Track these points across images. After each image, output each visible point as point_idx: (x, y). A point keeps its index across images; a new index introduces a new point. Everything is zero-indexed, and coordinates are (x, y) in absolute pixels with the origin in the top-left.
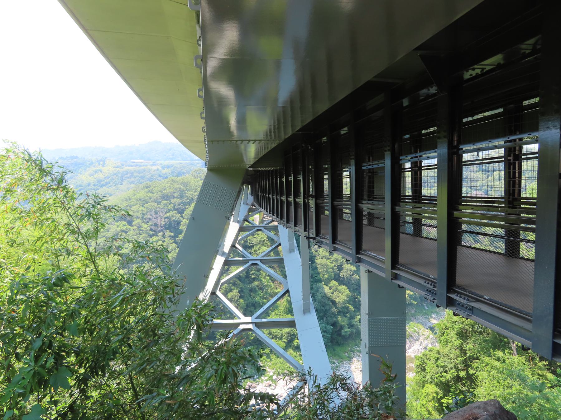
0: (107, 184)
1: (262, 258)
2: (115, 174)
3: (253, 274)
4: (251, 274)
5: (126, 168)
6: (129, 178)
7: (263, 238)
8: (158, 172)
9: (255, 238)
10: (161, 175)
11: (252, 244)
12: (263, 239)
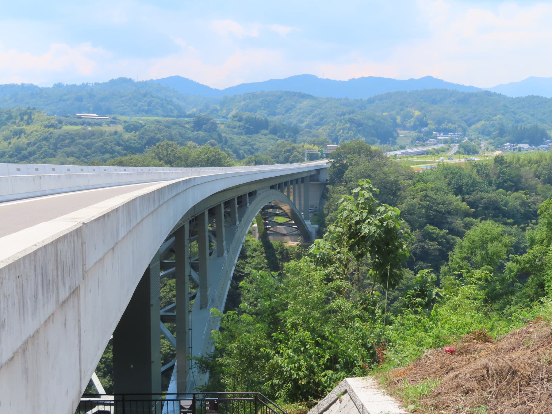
0: (31, 154)
1: (164, 314)
2: (46, 139)
5: (67, 128)
6: (66, 146)
8: (116, 137)
9: (247, 263)
10: (121, 142)
11: (242, 272)
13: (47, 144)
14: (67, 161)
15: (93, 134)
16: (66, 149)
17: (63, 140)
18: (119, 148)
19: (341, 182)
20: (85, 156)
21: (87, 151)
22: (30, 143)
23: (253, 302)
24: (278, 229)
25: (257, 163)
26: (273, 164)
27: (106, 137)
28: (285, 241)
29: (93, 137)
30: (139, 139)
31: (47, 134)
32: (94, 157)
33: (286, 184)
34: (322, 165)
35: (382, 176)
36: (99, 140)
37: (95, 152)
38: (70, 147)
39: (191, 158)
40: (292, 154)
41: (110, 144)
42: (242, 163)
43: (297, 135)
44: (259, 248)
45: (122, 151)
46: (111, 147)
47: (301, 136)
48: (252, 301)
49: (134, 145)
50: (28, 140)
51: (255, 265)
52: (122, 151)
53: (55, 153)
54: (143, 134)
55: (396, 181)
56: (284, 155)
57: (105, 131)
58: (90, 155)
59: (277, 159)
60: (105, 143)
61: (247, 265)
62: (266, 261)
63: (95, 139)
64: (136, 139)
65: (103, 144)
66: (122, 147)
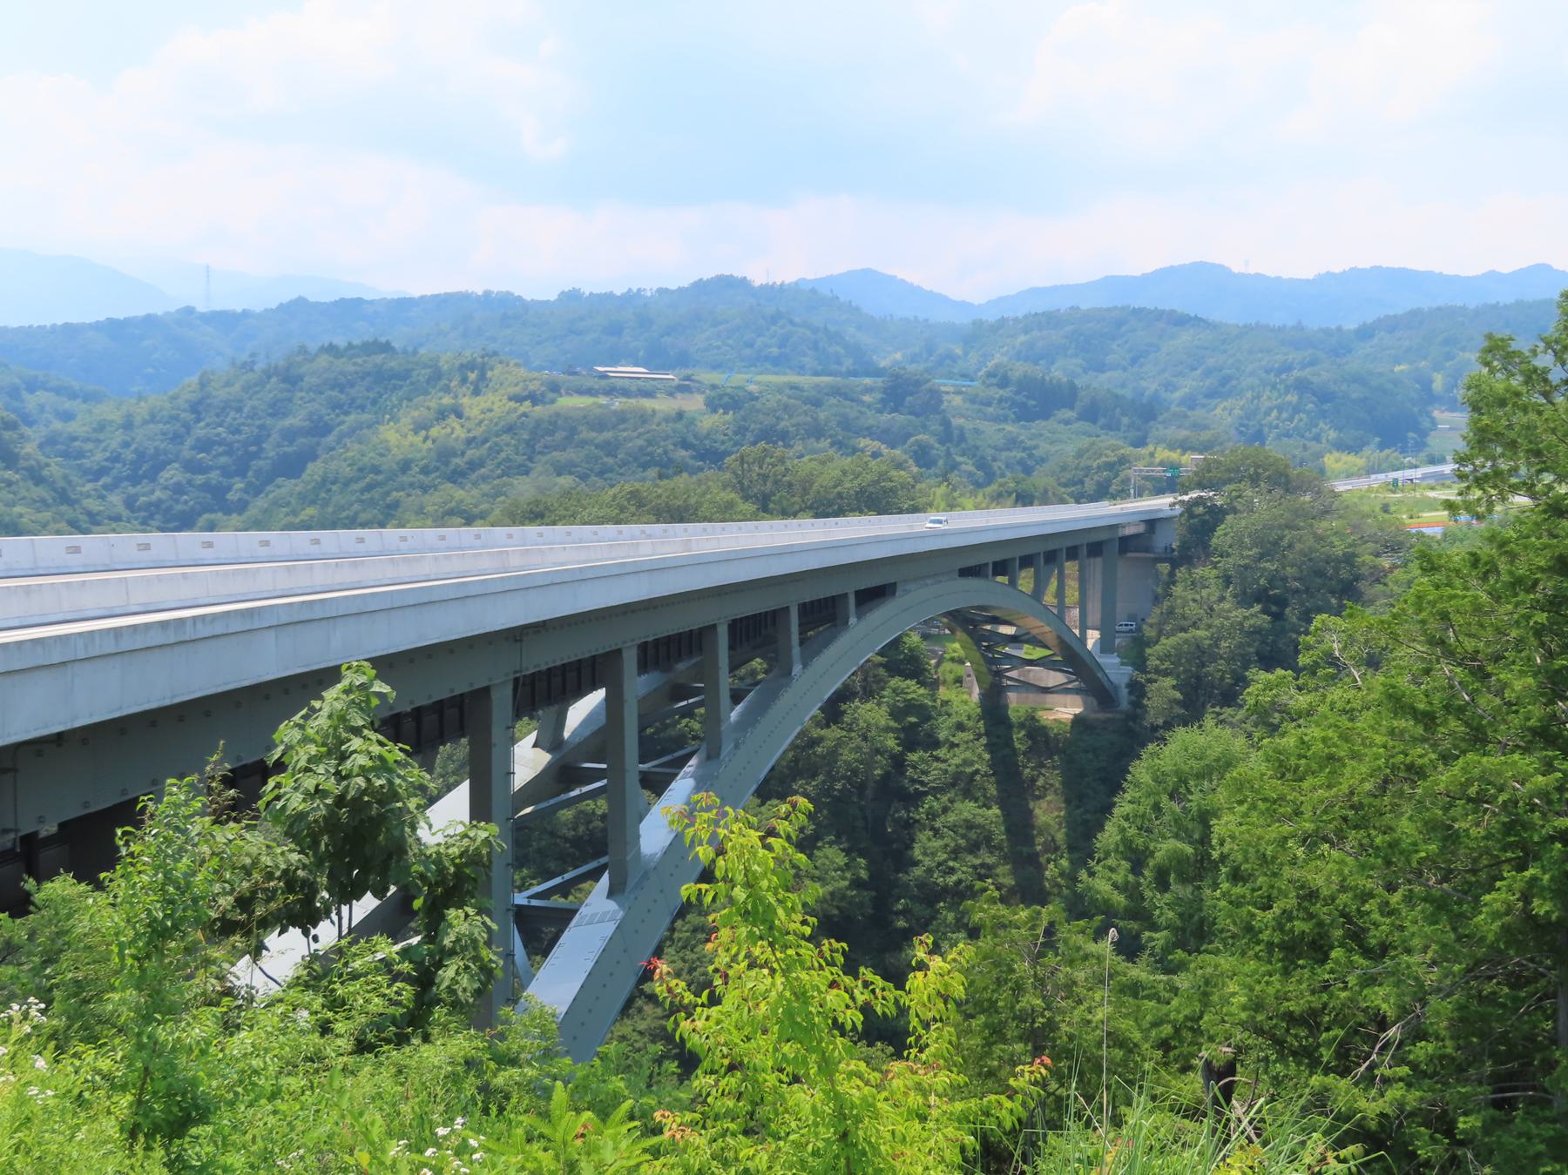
0: (473, 466)
2: (510, 429)
3: (905, 912)
4: (898, 913)
5: (569, 403)
6: (556, 448)
7: (972, 763)
8: (679, 426)
9: (937, 759)
10: (691, 439)
11: (922, 783)
12: (969, 770)
13: (513, 442)
14: (556, 484)
15: (621, 417)
16: (555, 454)
17: (551, 433)
18: (684, 453)
19: (1208, 555)
20: (601, 474)
21: (606, 459)
22: (474, 438)
23: (945, 861)
24: (1031, 674)
25: (1024, 499)
26: (1062, 501)
27: (654, 427)
28: (1047, 706)
29: (622, 426)
30: (736, 433)
31: (514, 416)
32: (622, 474)
33: (1051, 557)
34: (1160, 510)
35: (1311, 542)
36: (635, 434)
37: (624, 464)
38: (564, 450)
39: (816, 487)
40: (1116, 476)
41: (662, 443)
42: (980, 497)
43: (1152, 423)
44: (971, 724)
45: (691, 462)
46: (666, 452)
47: (1160, 426)
48: (941, 859)
49: (723, 447)
50: (469, 431)
51: (957, 766)
52: (691, 462)
53: (530, 464)
54: (745, 421)
55: (1349, 559)
56: (1096, 478)
57: (654, 411)
58: (611, 470)
59: (1079, 487)
60: (650, 443)
61: (935, 764)
62: (987, 756)
63: (624, 430)
64: (730, 432)
65: (645, 444)
66: (690, 452)
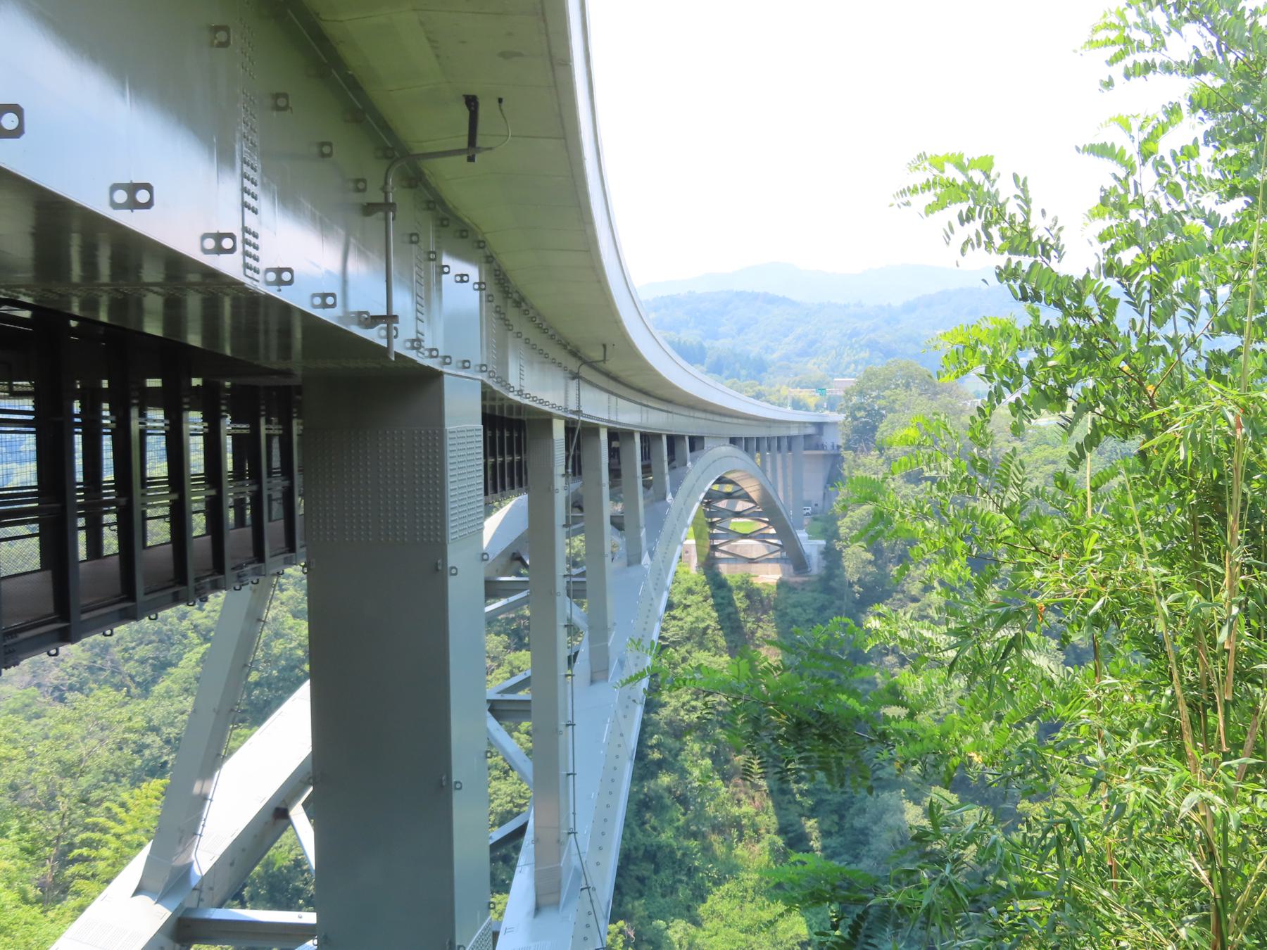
1: (499, 697)
3: (658, 746)
4: (652, 747)
7: (703, 620)
9: (674, 618)
12: (702, 625)
23: (688, 702)
43: (763, 374)
44: (698, 589)
47: (772, 377)
62: (715, 614)
